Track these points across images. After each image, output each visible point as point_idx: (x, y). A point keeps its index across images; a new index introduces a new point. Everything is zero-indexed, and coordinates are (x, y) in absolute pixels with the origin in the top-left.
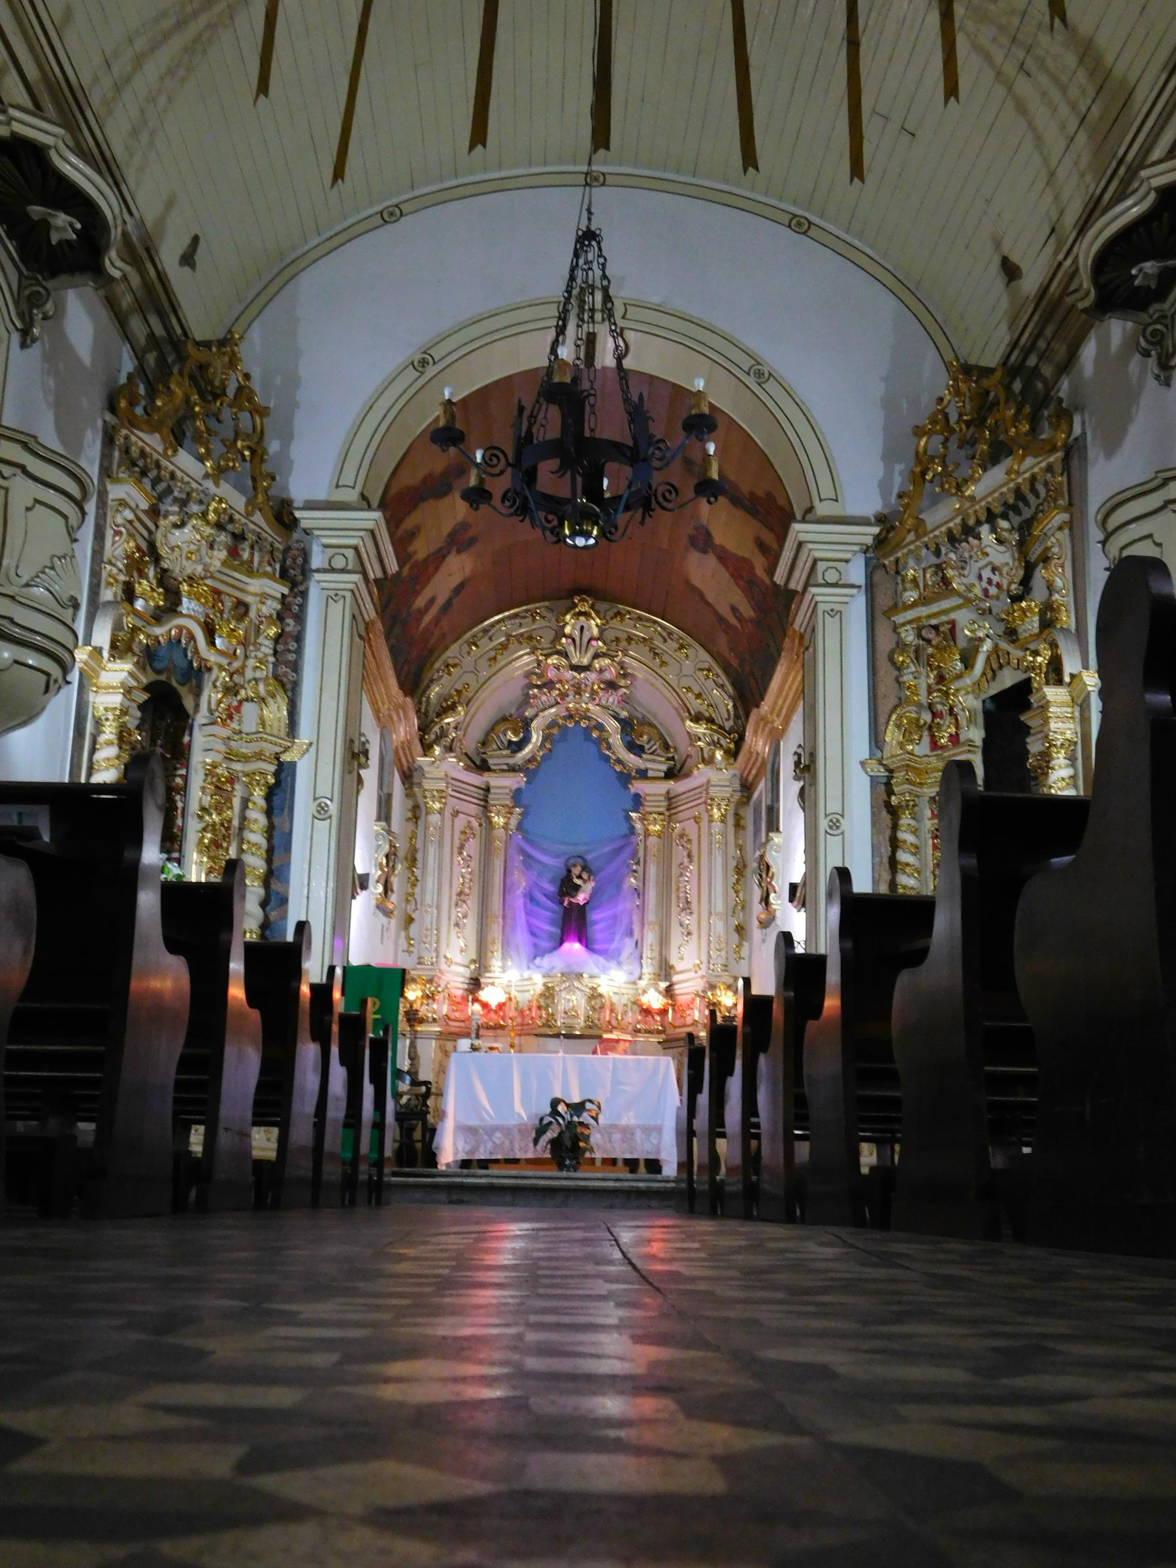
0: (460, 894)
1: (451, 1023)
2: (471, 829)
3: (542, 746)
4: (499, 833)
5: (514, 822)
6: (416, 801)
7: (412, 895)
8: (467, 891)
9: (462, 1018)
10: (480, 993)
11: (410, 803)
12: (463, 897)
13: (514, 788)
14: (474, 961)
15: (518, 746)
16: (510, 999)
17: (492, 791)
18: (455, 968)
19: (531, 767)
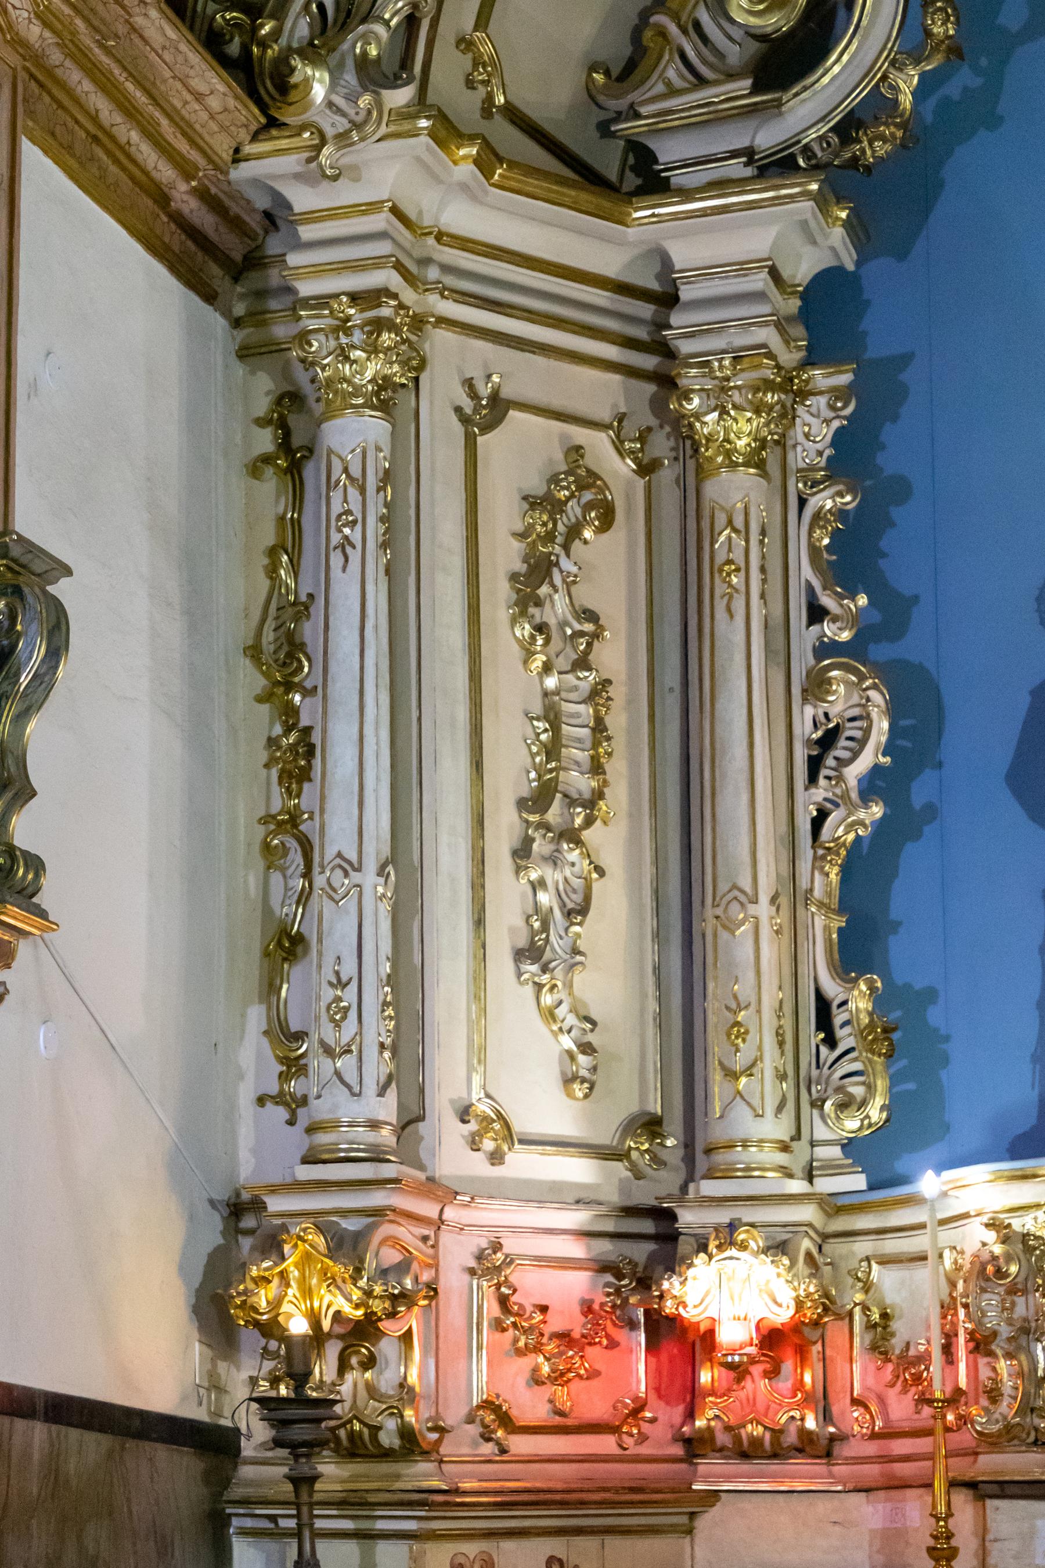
0: (538, 800)
1: (521, 1445)
2: (588, 480)
3: (912, 44)
4: (736, 489)
5: (815, 430)
6: (286, 373)
7: (292, 821)
8: (579, 782)
9: (598, 1409)
10: (671, 1285)
11: (262, 390)
12: (554, 814)
13: (803, 268)
14: (651, 1126)
15: (783, 63)
16: (828, 1305)
17: (686, 293)
18: (522, 1164)
19: (874, 149)
